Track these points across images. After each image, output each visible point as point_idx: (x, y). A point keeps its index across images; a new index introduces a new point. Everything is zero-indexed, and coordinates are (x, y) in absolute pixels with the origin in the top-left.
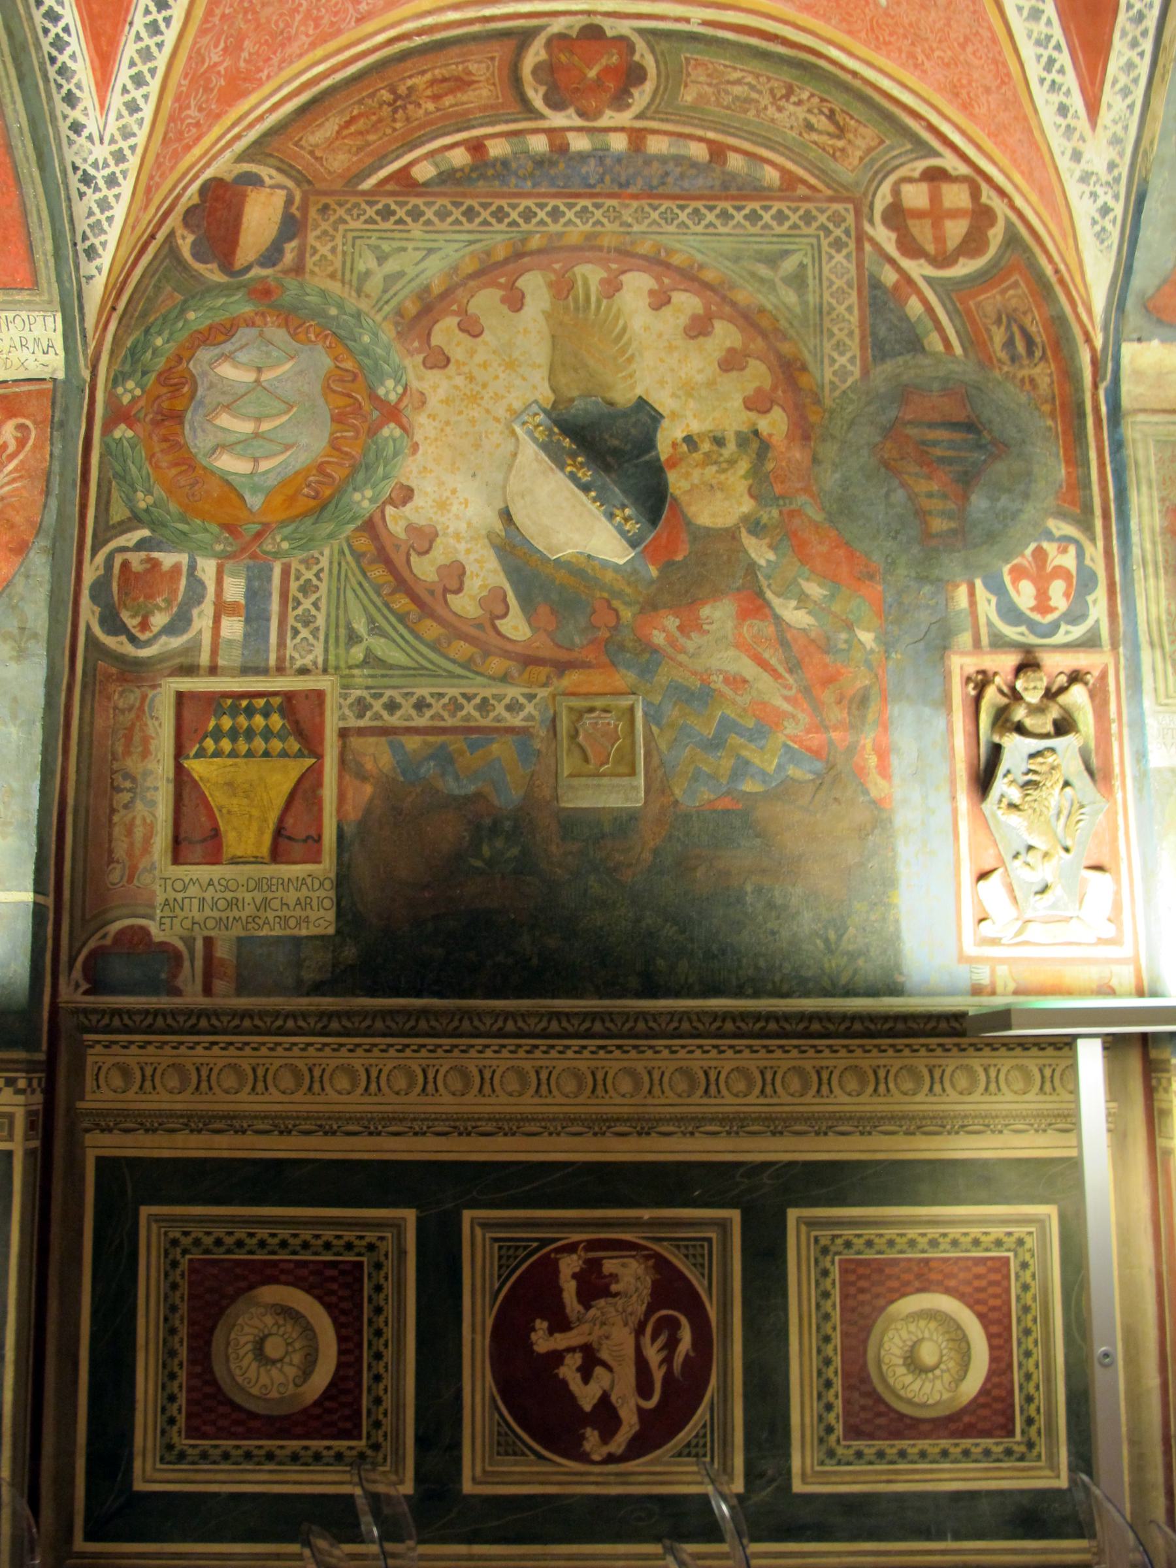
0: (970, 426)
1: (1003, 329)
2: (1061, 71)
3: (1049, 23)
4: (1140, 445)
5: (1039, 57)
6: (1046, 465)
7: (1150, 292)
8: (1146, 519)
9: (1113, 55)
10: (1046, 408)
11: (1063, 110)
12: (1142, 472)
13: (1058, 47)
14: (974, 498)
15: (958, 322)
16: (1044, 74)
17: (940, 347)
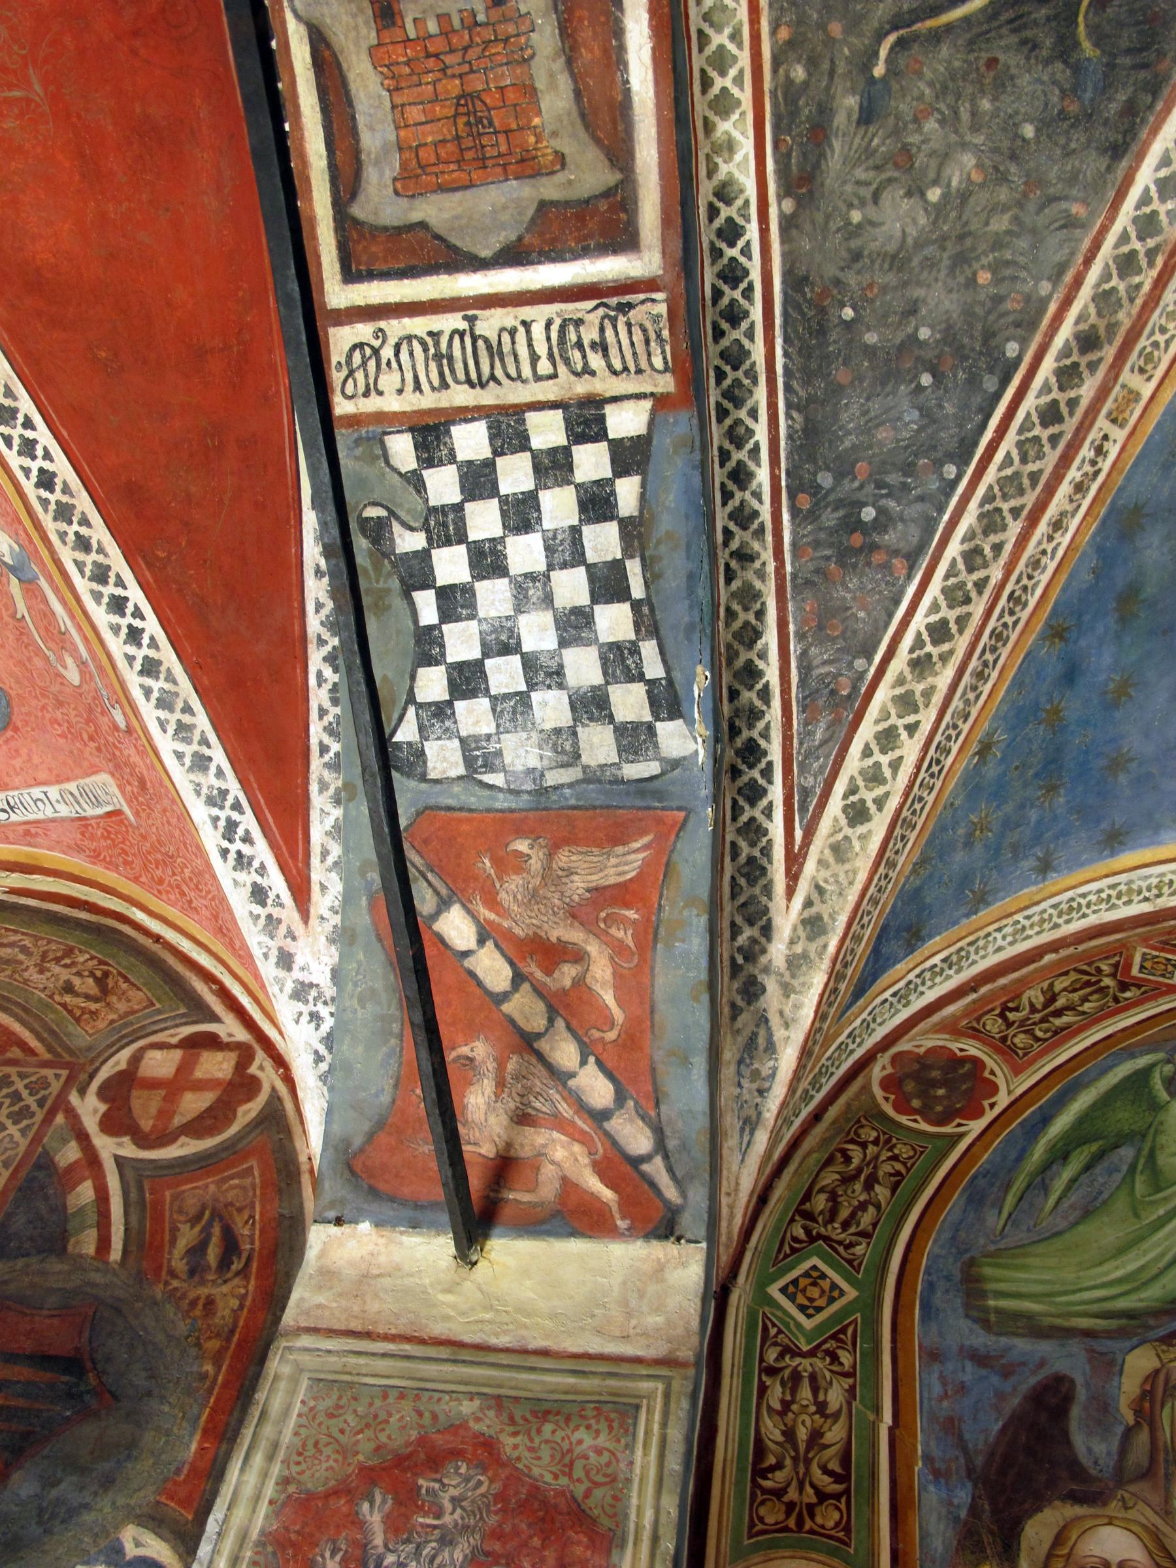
0: (73, 1364)
1: (197, 1229)
2: (247, 839)
3: (220, 773)
4: (282, 1385)
5: (215, 820)
6: (168, 1433)
7: (357, 1142)
8: (240, 1514)
9: (314, 815)
10: (213, 1345)
11: (259, 894)
12: (268, 1430)
13: (237, 806)
14: (16, 1476)
15: (134, 1219)
16: (225, 844)
17: (90, 1249)
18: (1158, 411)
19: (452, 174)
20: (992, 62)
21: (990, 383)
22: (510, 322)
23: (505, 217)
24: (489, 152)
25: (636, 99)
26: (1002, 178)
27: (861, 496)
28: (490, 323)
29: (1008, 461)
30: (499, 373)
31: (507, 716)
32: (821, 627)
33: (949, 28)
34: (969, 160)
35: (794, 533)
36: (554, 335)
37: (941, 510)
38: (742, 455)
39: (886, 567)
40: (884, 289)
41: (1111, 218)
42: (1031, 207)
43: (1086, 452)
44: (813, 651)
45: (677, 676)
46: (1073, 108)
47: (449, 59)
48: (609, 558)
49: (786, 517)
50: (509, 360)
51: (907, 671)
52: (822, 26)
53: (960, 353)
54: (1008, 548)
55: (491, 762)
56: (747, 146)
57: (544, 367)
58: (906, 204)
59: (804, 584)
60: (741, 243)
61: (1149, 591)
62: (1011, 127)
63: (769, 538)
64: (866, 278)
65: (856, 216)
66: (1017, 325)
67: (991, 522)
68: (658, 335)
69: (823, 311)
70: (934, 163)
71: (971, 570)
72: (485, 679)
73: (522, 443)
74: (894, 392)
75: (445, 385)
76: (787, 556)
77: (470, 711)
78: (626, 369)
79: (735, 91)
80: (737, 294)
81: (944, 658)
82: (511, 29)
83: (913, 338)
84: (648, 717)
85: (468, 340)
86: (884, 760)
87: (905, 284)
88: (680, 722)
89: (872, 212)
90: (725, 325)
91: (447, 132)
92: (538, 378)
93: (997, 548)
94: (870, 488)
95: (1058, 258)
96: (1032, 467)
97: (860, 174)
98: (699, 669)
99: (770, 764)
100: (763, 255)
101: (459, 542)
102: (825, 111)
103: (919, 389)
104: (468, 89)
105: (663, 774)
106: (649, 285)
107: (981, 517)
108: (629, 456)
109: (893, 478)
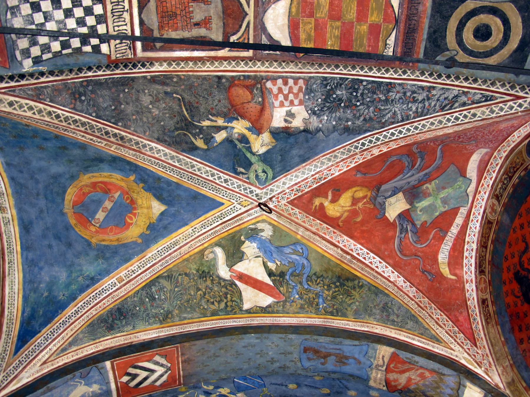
18: (107, 151)
19: (160, 10)
20: (175, 116)
21: (113, 120)
22: (127, 20)
23: (150, 21)
24: (164, 19)
25: (173, 53)
26: (153, 119)
27: (87, 96)
28: (126, 16)
29: (97, 126)
30: (115, 17)
31: (27, 18)
32: (56, 90)
33: (182, 108)
34: (157, 113)
35: (77, 82)
36: (124, 31)
37: (85, 113)
38: (95, 69)
39: (72, 103)
40: (132, 97)
41: (146, 140)
42: (148, 125)
43: (99, 140)
44: (50, 89)
45: (44, 63)
46: (166, 131)
47: (184, 12)
48: (72, 45)
49: (81, 80)
50: (117, 20)
51: (48, 111)
52: (183, 84)
53: (118, 114)
54: (78, 128)
55: (13, 14)
56: (161, 69)
57: (116, 29)
58: (149, 101)
59: (66, 85)
60: (141, 67)
61: (66, 152)
62: (163, 120)
63: (76, 76)
64: (134, 94)
65: (146, 91)
66: (125, 125)
67: (83, 124)
68: (124, 56)
69: (127, 85)
70: (156, 106)
71: (73, 121)
72: (37, 12)
73: (99, 22)
74: (110, 101)
75: (112, 3)
76: (72, 81)
77: (27, 8)
78: (116, 48)
79: (172, 67)
80: (130, 67)
81: (52, 118)
82: (189, 27)
83: (121, 104)
84: (32, 56)
85: (122, 10)
86: (26, 108)
87: (133, 102)
88: (32, 64)
89: (147, 94)
90: (124, 64)
91: (169, 10)
92: (114, 27)
93: (78, 126)
94: (89, 98)
95: (138, 131)
96: (96, 131)
97: (155, 92)
98: (46, 68)
99: (20, 81)
100: (139, 72)
101: (73, 5)
102: (167, 85)
103: (111, 106)
104: (178, 16)
105: (18, 61)
106: (135, 54)
107: (85, 122)
108: (96, 49)
109: (91, 103)
